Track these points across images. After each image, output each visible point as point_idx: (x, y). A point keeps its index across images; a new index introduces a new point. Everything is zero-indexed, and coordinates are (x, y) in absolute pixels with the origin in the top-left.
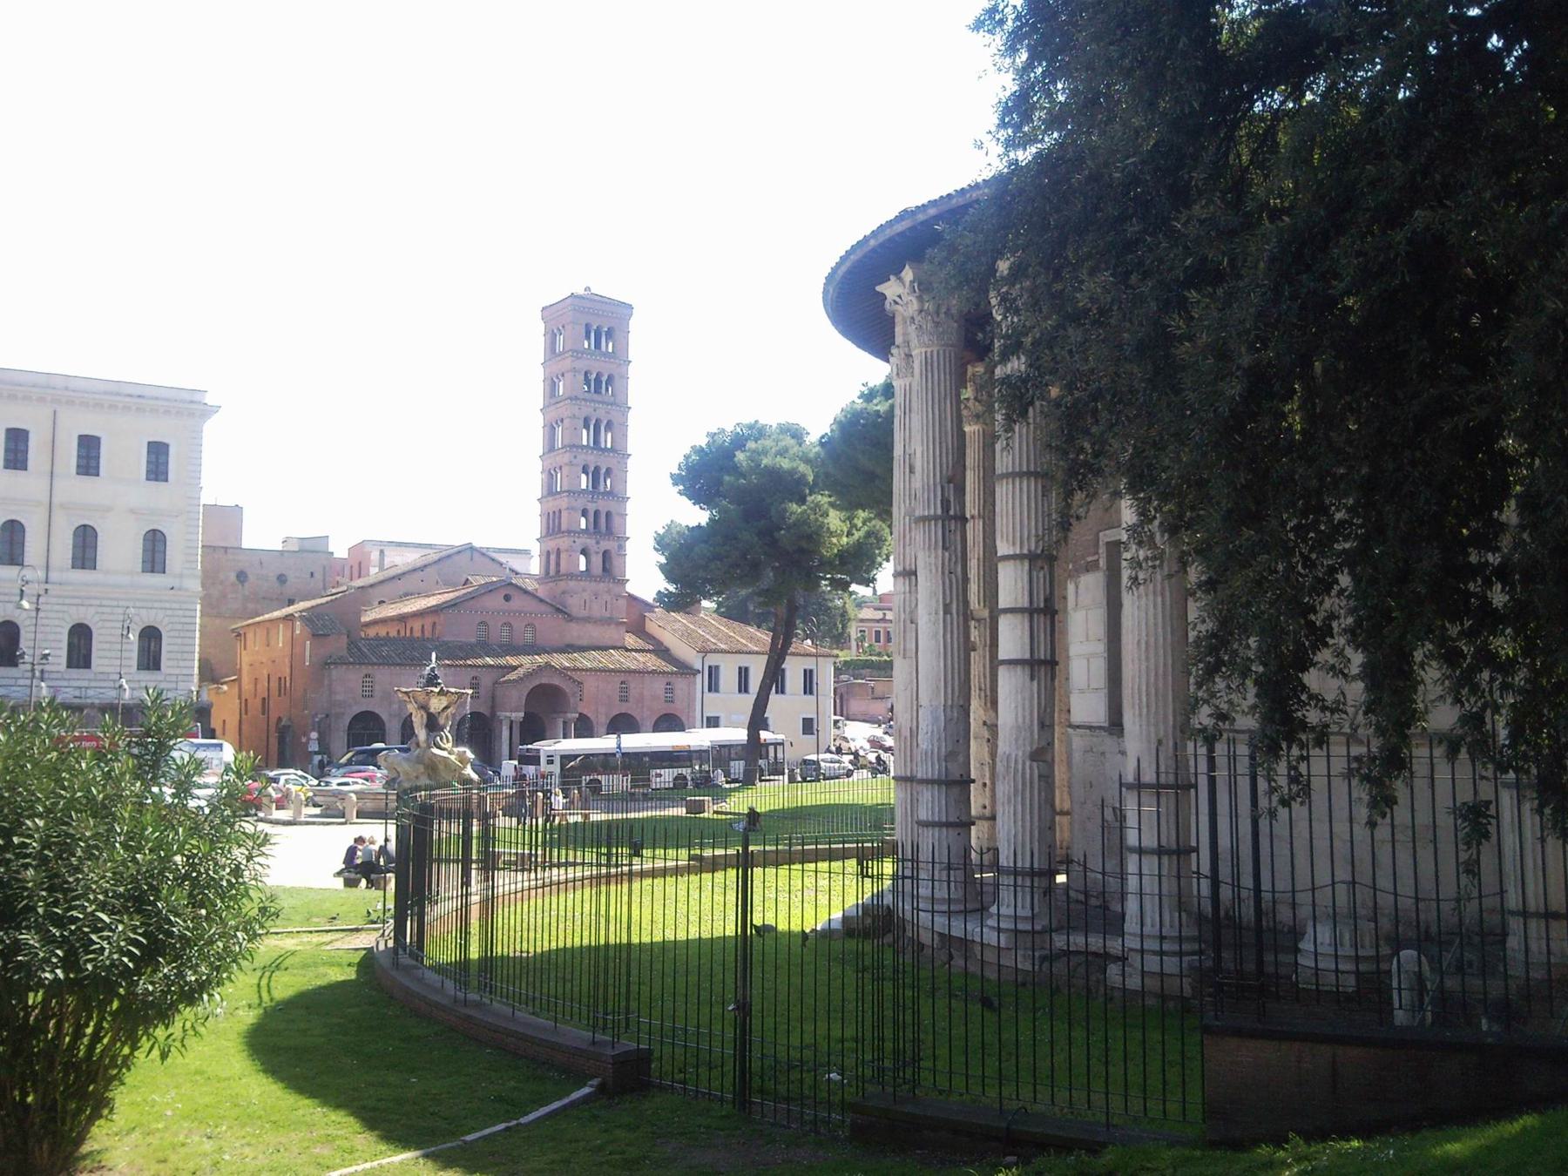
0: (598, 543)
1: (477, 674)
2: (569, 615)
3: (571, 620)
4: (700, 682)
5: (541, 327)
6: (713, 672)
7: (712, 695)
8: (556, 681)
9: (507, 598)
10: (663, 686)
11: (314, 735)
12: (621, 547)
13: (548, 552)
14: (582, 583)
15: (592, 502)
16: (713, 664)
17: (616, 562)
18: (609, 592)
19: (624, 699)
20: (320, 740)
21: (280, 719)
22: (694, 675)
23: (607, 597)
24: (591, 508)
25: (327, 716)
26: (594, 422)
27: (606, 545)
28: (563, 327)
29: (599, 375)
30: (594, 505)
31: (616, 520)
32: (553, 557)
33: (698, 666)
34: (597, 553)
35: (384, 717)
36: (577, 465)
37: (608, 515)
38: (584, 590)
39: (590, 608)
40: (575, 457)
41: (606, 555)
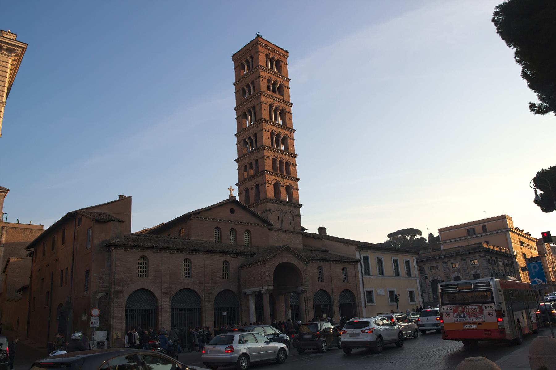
1: (226, 260)
3: (272, 229)
4: (360, 267)
5: (233, 65)
6: (366, 259)
7: (368, 277)
8: (292, 260)
9: (232, 211)
10: (341, 271)
11: (96, 312)
13: (247, 191)
14: (276, 205)
16: (365, 255)
19: (321, 279)
20: (101, 317)
21: (61, 304)
22: (357, 262)
25: (107, 294)
26: (274, 108)
28: (251, 57)
29: (275, 83)
31: (291, 167)
33: (358, 257)
35: (157, 294)
39: (282, 222)
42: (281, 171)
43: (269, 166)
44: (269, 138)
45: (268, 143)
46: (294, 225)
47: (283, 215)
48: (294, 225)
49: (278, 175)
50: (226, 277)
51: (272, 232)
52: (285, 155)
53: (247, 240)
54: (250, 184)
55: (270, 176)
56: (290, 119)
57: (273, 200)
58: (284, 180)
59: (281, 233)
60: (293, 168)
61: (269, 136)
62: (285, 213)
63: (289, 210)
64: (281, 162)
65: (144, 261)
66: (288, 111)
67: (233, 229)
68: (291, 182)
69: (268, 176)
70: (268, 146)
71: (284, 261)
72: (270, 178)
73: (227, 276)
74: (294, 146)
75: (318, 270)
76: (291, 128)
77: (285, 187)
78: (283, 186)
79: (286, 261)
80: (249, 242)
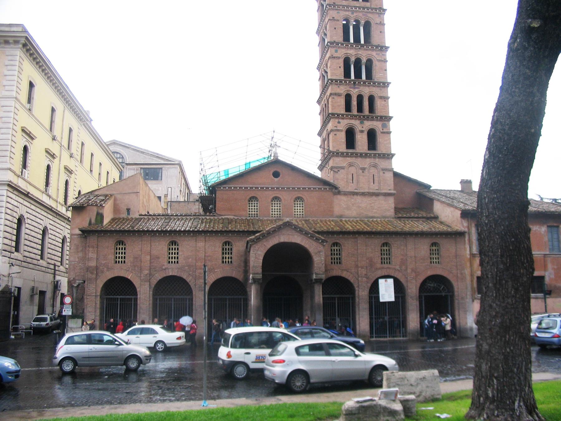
0: (362, 123)
2: (336, 188)
3: (339, 193)
8: (297, 239)
12: (385, 126)
15: (355, 88)
17: (380, 139)
18: (375, 166)
23: (373, 170)
24: (354, 93)
27: (368, 125)
30: (356, 90)
31: (378, 103)
32: (326, 143)
34: (362, 132)
36: (339, 58)
37: (371, 99)
38: (351, 165)
39: (358, 182)
40: (336, 51)
41: (372, 136)
42: (360, 108)
43: (339, 106)
44: (340, 67)
45: (337, 75)
46: (379, 183)
47: (361, 171)
48: (379, 183)
49: (354, 117)
50: (228, 261)
51: (339, 196)
52: (369, 86)
53: (300, 209)
54: (324, 134)
55: (340, 120)
56: (381, 32)
57: (342, 153)
58: (365, 122)
59: (355, 197)
60: (383, 103)
61: (342, 65)
62: (363, 169)
63: (372, 164)
64: (360, 98)
65: (122, 246)
66: (378, 22)
67: (250, 198)
68: (378, 123)
69: (337, 120)
70: (340, 78)
71: (282, 240)
72: (339, 123)
73: (230, 260)
74: (386, 70)
75: (385, 248)
76: (383, 45)
77: (366, 133)
78: (362, 132)
79: (286, 240)
80: (302, 212)
